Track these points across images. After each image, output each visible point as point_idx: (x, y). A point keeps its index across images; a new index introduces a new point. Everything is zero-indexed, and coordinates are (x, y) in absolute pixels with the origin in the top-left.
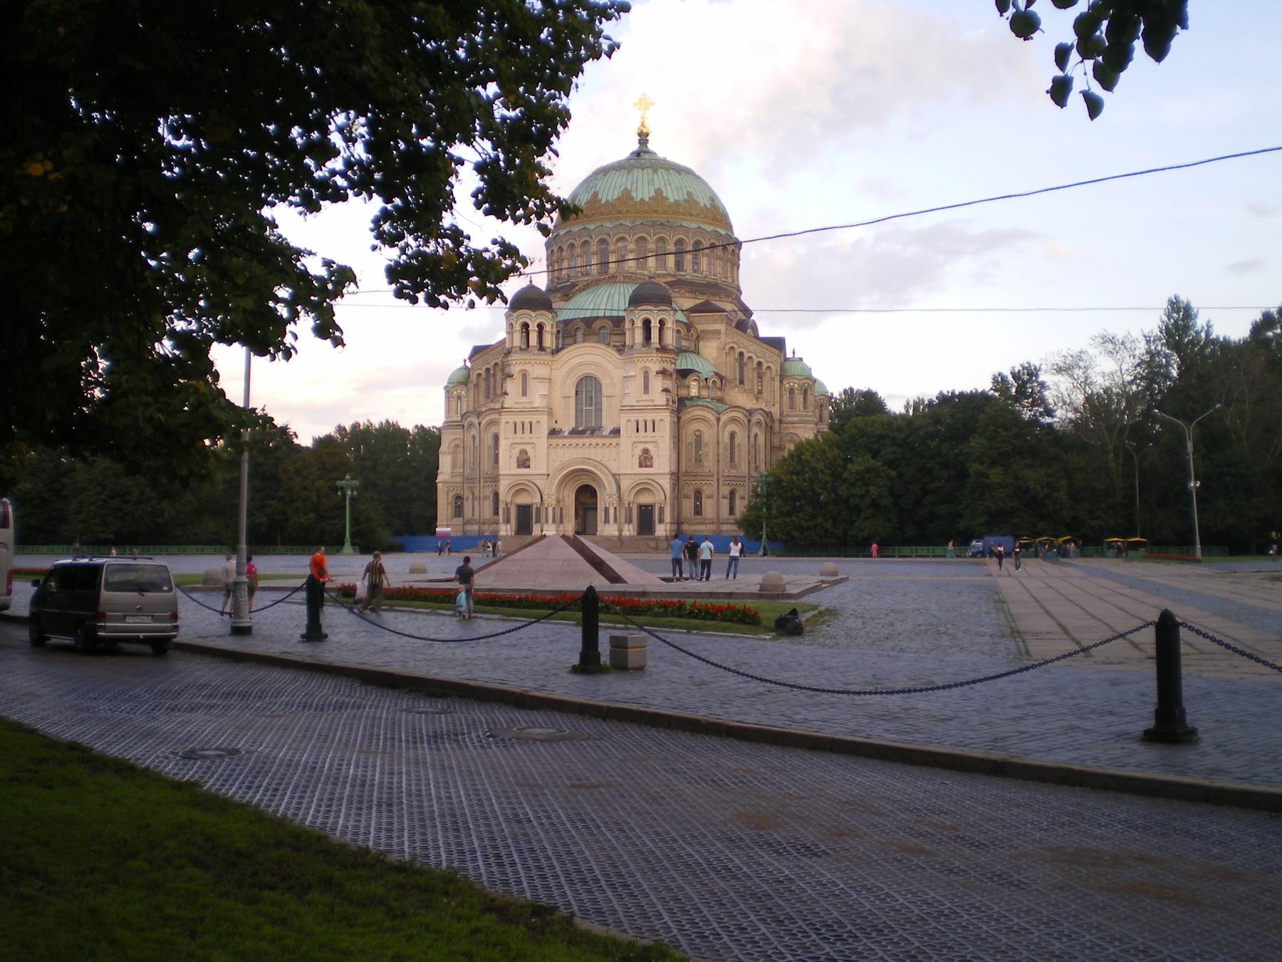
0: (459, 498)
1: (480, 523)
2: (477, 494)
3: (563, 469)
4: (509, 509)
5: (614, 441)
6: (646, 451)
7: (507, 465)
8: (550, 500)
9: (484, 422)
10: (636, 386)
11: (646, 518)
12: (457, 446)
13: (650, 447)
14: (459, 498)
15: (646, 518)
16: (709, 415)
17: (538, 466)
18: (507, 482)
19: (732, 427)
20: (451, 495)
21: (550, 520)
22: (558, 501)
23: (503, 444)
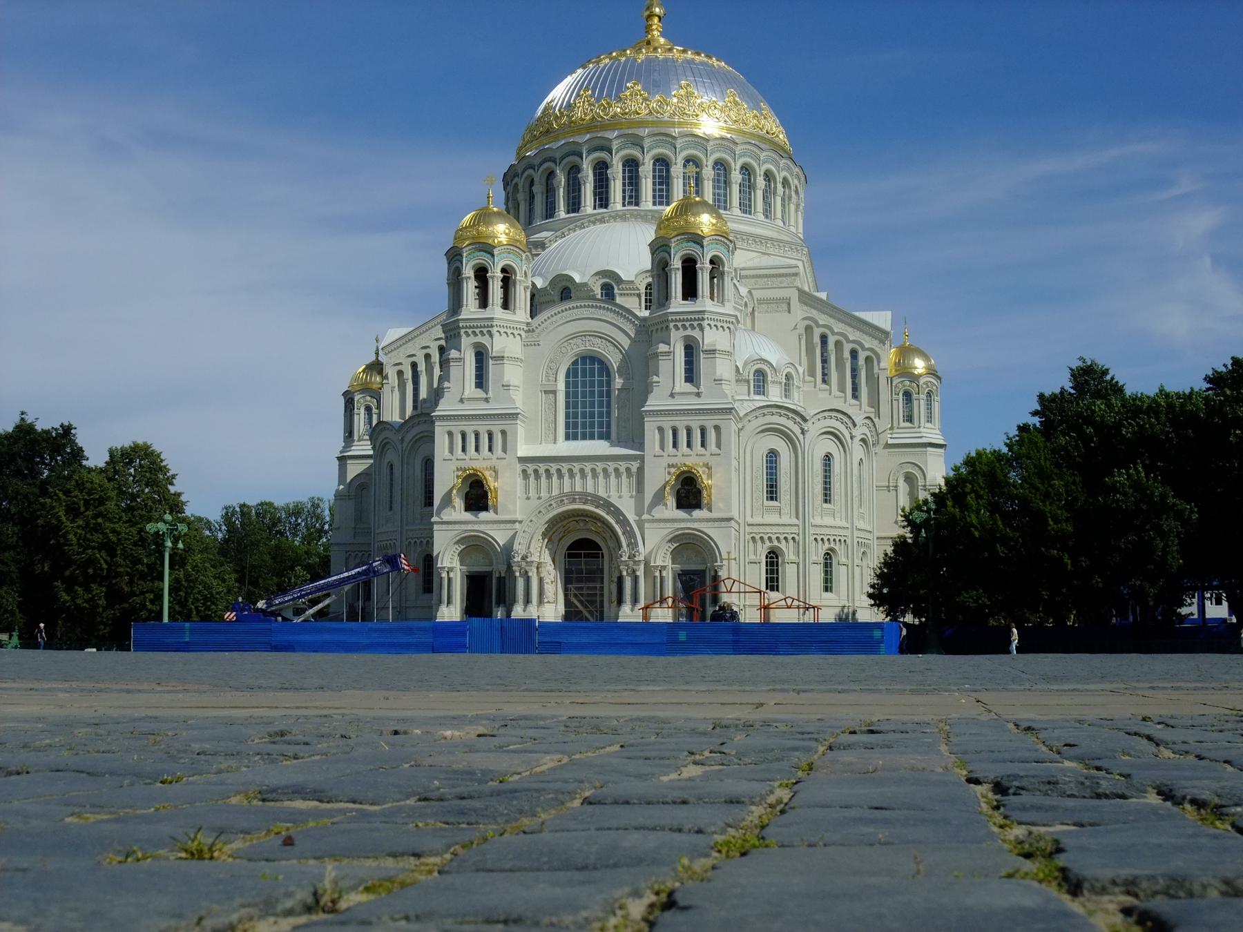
4: (449, 579)
16: (790, 424)
19: (830, 446)
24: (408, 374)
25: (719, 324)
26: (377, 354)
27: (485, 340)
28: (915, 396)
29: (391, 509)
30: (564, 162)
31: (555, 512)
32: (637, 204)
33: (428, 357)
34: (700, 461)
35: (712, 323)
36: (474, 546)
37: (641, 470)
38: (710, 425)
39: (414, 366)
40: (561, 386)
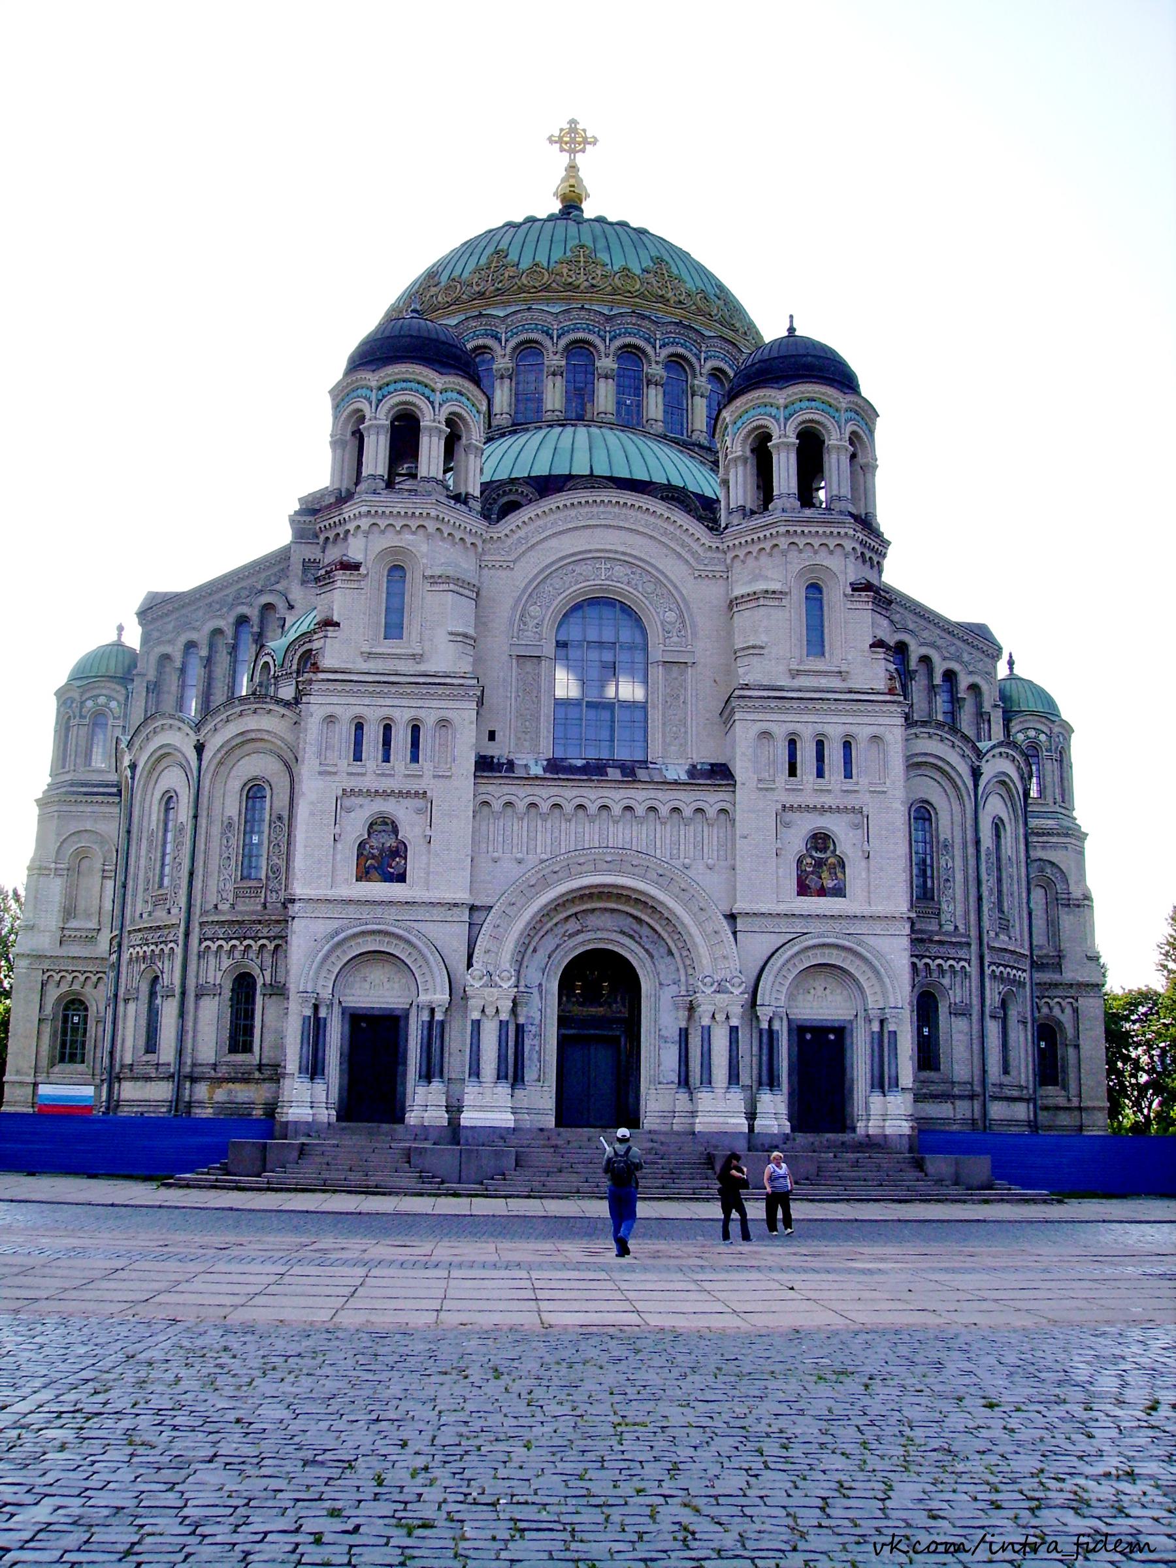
0: (74, 1005)
1: (185, 1076)
2: (172, 976)
3: (545, 882)
5: (712, 800)
6: (820, 840)
7: (319, 866)
8: (491, 997)
9: (214, 744)
10: (776, 634)
11: (817, 1069)
12: (82, 855)
13: (836, 826)
14: (74, 1005)
15: (817, 1069)
16: (954, 758)
17: (440, 872)
18: (322, 928)
20: (53, 994)
23: (315, 793)
34: (850, 801)
38: (863, 733)
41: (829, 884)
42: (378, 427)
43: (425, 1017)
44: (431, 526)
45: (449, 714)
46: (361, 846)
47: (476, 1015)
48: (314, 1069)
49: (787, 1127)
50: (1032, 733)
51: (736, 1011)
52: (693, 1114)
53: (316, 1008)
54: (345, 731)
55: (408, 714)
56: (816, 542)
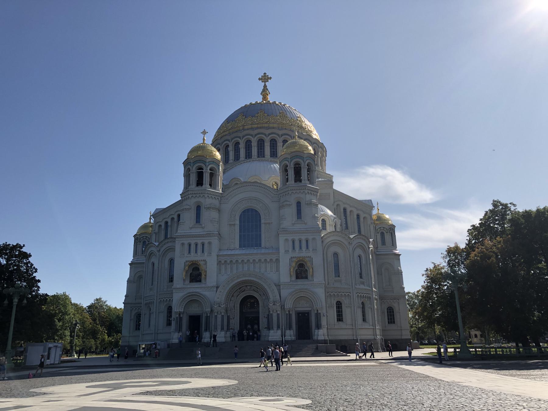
4: (181, 319)
12: (140, 277)
21: (219, 327)
22: (227, 311)
24: (163, 227)
25: (312, 193)
26: (150, 219)
27: (201, 200)
28: (385, 234)
29: (152, 284)
30: (233, 141)
31: (236, 282)
32: (264, 157)
33: (173, 219)
35: (310, 192)
36: (193, 300)
37: (278, 260)
38: (310, 238)
39: (166, 223)
40: (238, 222)
41: (304, 276)
42: (193, 173)
43: (206, 315)
44: (206, 196)
45: (210, 240)
46: (191, 274)
47: (216, 314)
48: (179, 329)
49: (293, 338)
50: (382, 228)
51: (279, 309)
52: (269, 336)
53: (180, 314)
54: (186, 247)
55: (201, 241)
56: (298, 191)
